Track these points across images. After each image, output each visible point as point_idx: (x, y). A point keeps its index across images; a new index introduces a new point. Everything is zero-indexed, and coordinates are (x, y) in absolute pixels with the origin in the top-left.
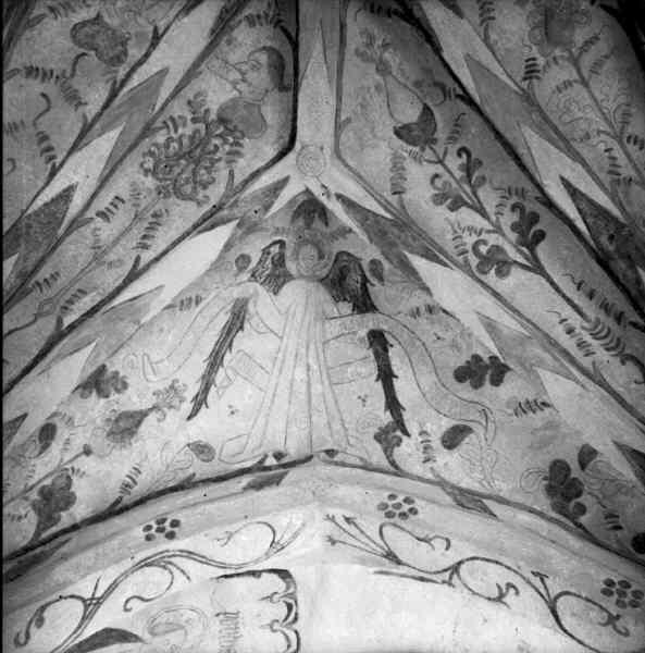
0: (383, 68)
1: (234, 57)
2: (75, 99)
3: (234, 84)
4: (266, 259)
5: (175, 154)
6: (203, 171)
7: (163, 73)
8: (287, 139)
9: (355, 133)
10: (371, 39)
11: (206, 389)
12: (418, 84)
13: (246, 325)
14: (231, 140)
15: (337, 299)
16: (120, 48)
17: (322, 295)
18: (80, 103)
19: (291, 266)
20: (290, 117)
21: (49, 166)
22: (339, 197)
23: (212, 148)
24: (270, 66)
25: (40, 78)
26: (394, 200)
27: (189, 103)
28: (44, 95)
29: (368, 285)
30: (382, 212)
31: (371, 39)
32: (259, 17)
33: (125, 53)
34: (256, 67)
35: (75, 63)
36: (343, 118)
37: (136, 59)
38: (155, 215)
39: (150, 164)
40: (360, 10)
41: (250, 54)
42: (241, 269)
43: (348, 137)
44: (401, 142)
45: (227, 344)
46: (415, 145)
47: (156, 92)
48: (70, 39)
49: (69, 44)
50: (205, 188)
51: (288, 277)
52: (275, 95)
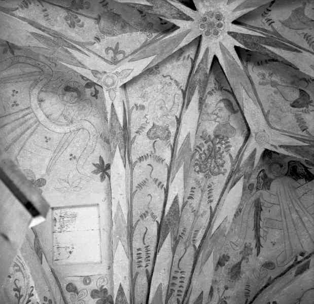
0: (274, 84)
1: (210, 111)
2: (160, 160)
3: (215, 120)
4: (259, 180)
5: (205, 159)
6: (219, 160)
7: (188, 136)
8: (246, 130)
9: (274, 115)
10: (263, 75)
11: (259, 241)
12: (293, 83)
13: (263, 208)
14: (223, 142)
15: (296, 179)
16: (167, 132)
17: (289, 180)
18: (163, 161)
19: (270, 176)
20: (243, 121)
21: (163, 190)
22: (281, 146)
23: (218, 149)
24: (225, 106)
25: (145, 160)
26: (304, 133)
27: (201, 137)
28: (149, 165)
29: (309, 170)
30: (301, 143)
31: (263, 75)
32: (213, 90)
33: (169, 132)
34: (220, 110)
35: (154, 146)
36: (266, 111)
37: (174, 133)
38: (209, 187)
39: (198, 169)
40: (253, 67)
41: (217, 105)
42: (251, 190)
43: (271, 117)
44: (296, 109)
45: (259, 218)
46: (303, 107)
47: (189, 144)
48: (148, 139)
49: (148, 141)
50: (222, 166)
51: (271, 180)
52: (232, 117)
